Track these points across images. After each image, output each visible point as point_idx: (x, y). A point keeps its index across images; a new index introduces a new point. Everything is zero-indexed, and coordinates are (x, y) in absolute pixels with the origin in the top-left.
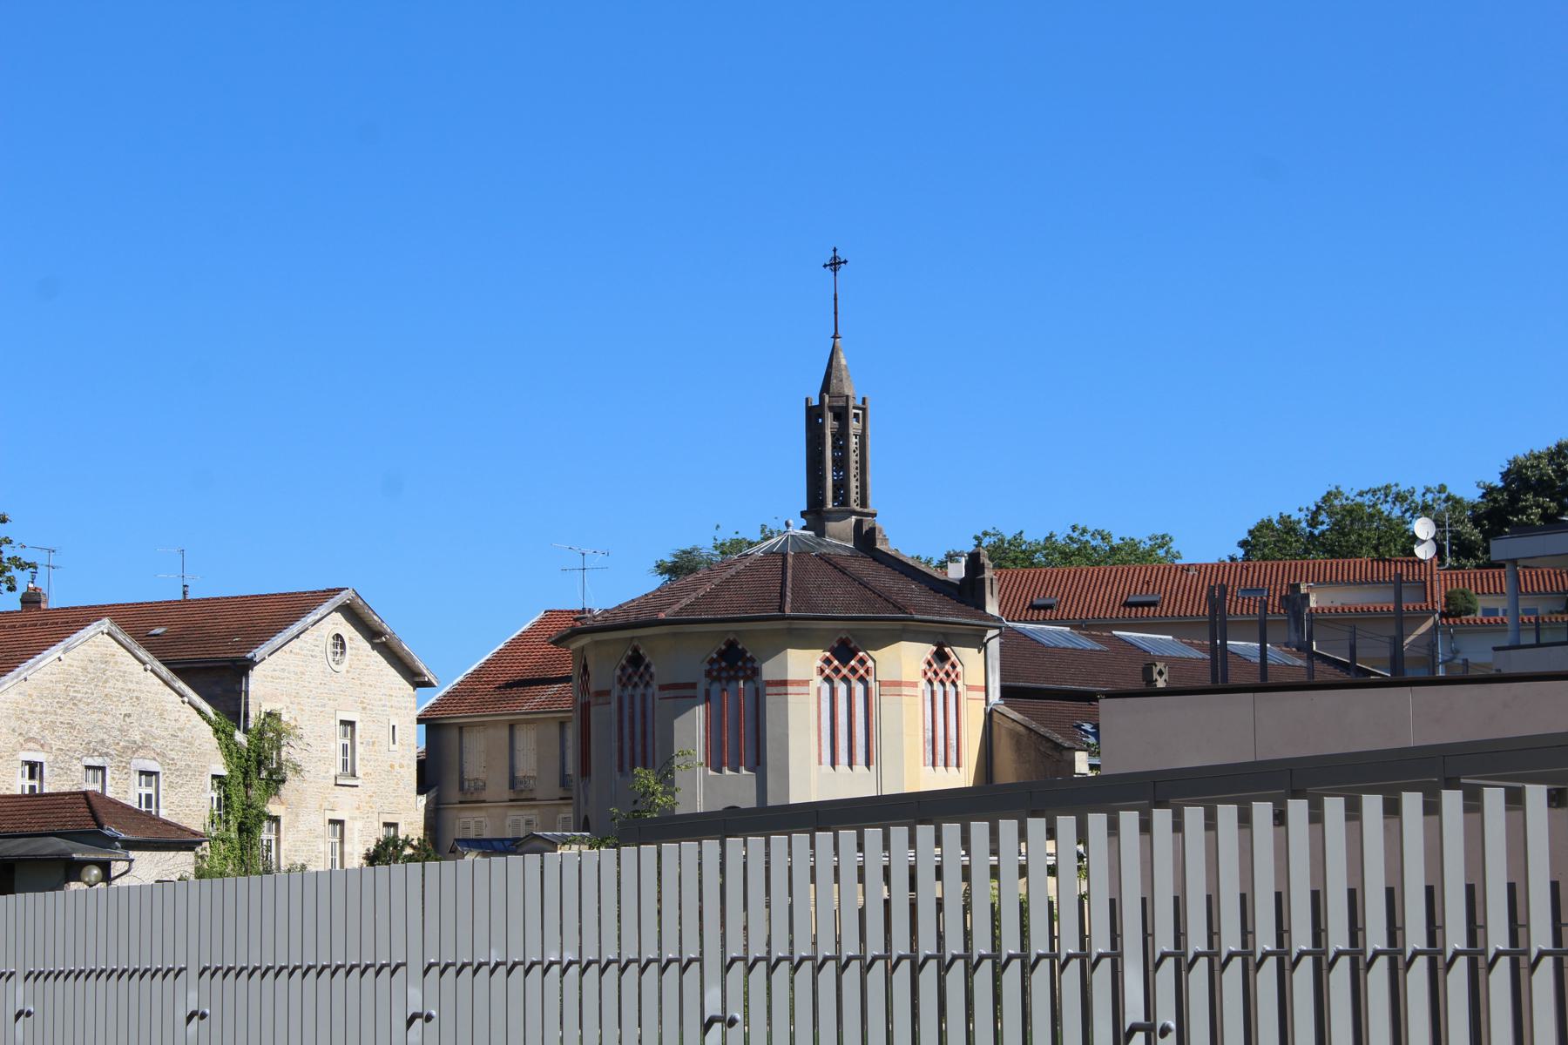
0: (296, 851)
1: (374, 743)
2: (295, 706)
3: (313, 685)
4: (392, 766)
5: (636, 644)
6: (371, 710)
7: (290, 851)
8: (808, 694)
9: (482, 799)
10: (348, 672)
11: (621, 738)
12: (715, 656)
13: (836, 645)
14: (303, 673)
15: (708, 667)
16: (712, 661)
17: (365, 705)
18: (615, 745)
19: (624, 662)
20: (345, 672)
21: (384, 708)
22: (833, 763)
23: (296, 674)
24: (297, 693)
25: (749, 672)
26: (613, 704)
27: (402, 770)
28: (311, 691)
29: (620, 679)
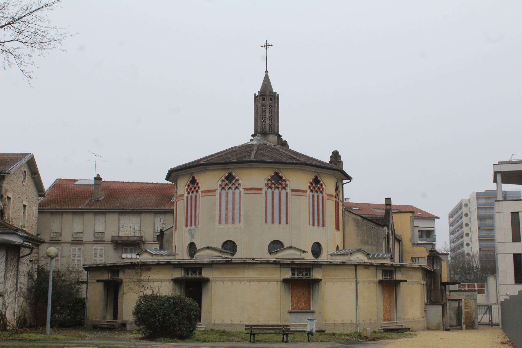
4: (32, 225)
5: (230, 171)
8: (306, 196)
11: (220, 210)
12: (270, 178)
13: (314, 178)
15: (266, 182)
16: (269, 180)
18: (217, 212)
19: (223, 178)
22: (313, 225)
25: (284, 185)
26: (216, 196)
29: (221, 185)
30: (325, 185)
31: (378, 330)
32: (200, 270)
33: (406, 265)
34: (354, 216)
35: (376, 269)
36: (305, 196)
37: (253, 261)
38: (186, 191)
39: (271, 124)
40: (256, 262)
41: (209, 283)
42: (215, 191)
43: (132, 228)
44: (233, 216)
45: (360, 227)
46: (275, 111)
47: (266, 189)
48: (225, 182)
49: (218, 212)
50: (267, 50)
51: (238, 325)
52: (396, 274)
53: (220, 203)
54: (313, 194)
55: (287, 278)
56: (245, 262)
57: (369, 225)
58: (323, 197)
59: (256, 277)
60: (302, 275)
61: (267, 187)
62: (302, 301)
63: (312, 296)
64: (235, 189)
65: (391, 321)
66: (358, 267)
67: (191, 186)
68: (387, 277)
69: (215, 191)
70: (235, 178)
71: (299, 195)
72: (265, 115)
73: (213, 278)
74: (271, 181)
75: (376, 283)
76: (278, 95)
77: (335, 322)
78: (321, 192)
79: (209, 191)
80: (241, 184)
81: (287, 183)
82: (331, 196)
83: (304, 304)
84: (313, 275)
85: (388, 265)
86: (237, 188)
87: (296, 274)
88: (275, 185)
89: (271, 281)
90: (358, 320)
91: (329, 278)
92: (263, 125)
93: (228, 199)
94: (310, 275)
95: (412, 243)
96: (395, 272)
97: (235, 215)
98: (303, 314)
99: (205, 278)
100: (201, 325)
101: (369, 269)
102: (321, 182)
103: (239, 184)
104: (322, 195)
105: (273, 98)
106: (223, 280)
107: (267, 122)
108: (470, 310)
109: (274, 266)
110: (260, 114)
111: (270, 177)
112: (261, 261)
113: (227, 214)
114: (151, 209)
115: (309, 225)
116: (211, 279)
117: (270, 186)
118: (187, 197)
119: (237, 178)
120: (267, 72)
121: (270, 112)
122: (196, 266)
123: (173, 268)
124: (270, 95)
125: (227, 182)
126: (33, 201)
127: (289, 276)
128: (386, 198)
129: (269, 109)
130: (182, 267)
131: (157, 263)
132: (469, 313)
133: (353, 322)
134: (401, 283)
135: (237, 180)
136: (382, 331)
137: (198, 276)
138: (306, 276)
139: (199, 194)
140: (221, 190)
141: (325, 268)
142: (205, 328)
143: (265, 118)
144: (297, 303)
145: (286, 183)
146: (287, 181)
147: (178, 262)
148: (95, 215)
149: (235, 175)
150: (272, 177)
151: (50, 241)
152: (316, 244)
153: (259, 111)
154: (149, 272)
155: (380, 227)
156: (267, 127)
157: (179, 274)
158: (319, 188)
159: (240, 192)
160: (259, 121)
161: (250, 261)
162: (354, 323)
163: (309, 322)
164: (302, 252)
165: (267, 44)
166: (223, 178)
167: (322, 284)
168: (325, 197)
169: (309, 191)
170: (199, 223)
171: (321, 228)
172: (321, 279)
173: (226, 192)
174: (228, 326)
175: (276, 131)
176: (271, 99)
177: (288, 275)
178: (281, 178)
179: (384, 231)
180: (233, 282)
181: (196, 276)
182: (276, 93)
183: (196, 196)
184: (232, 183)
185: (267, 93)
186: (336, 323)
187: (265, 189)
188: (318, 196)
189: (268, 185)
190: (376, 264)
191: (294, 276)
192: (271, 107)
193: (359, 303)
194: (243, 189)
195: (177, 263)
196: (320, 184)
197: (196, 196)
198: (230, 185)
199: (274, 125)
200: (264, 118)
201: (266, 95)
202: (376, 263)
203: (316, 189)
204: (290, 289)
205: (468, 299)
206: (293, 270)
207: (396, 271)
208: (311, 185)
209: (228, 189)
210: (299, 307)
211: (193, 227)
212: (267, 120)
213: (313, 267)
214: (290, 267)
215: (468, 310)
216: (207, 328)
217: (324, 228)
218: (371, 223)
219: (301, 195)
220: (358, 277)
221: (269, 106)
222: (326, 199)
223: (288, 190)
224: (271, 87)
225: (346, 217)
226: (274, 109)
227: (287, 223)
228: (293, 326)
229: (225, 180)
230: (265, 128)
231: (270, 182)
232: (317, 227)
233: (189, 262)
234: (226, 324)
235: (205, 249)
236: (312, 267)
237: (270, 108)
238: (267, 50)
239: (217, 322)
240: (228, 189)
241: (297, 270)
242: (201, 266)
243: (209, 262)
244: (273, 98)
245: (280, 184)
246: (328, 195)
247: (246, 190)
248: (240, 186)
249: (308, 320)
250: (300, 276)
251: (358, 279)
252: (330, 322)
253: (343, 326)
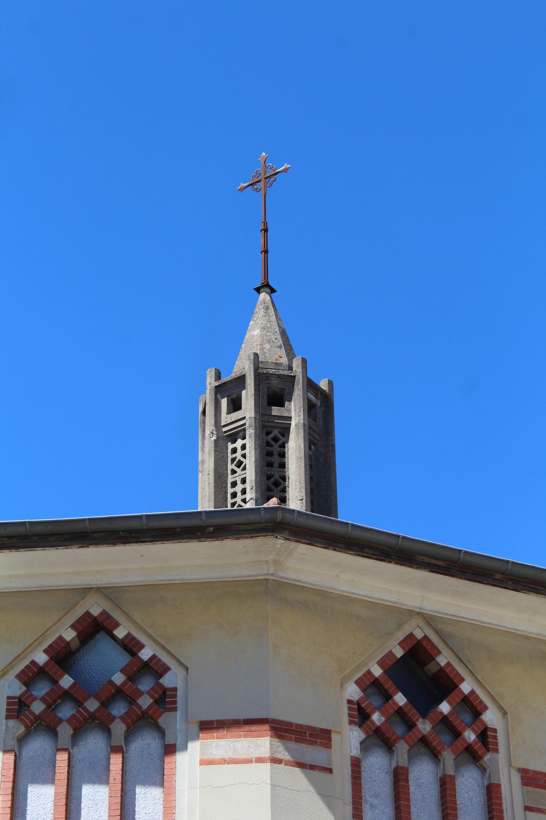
12: (41, 658)
13: (399, 653)
25: (145, 702)
54: (394, 765)
74: (55, 682)
81: (167, 681)
88: (79, 703)
111: (46, 651)
117: (38, 718)
145: (161, 681)
146: (168, 669)
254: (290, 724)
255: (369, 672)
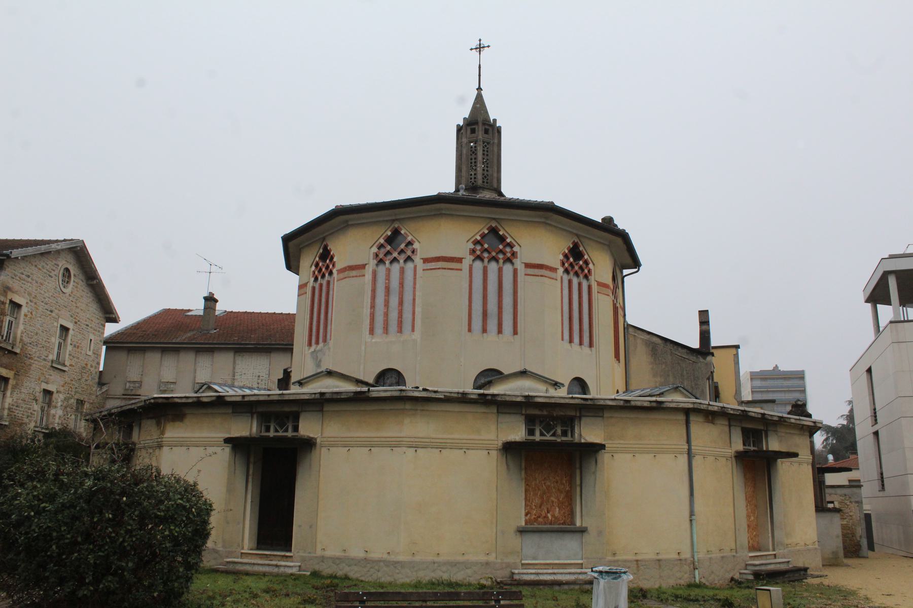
0: (17, 406)
1: (78, 347)
2: (33, 304)
3: (47, 295)
4: (86, 364)
5: (396, 226)
6: (79, 325)
7: (13, 405)
8: (556, 280)
9: (138, 394)
10: (70, 295)
11: (373, 306)
12: (479, 238)
13: (571, 246)
14: (42, 284)
15: (472, 246)
16: (476, 242)
17: (77, 321)
18: (367, 311)
19: (382, 241)
20: (68, 294)
21: (87, 327)
22: (571, 341)
23: (37, 282)
24: (36, 296)
25: (509, 255)
26: (367, 276)
27: (92, 369)
28: (45, 298)
29: (377, 255)
30: (594, 264)
31: (738, 574)
32: (296, 417)
33: (790, 418)
34: (647, 337)
35: (730, 426)
36: (553, 279)
37: (424, 394)
38: (311, 276)
39: (486, 173)
40: (434, 395)
41: (313, 449)
42: (363, 267)
43: (256, 376)
44: (399, 318)
45: (660, 359)
46: (493, 150)
47: (471, 263)
48: (385, 248)
49: (369, 310)
50: (480, 54)
51: (382, 564)
52: (769, 439)
53: (374, 291)
54: (569, 278)
55: (513, 440)
56: (404, 394)
57: (677, 353)
58: (590, 287)
59: (434, 436)
60: (554, 435)
61: (472, 258)
62: (553, 502)
63: (578, 489)
64: (405, 261)
65: (760, 550)
66: (692, 418)
67: (320, 264)
68: (749, 445)
69: (363, 267)
70: (406, 238)
71: (542, 276)
72: (475, 159)
73: (322, 440)
74: (482, 245)
75: (730, 459)
76: (500, 127)
77: (639, 557)
78: (586, 277)
79: (351, 268)
80: (418, 251)
81: (515, 249)
82: (606, 286)
83: (557, 509)
84: (580, 435)
85: (756, 416)
86: (409, 259)
87: (537, 433)
88: (489, 253)
89: (472, 449)
90: (695, 550)
91: (622, 442)
92: (471, 175)
93: (389, 283)
94: (572, 436)
95: (738, 401)
96: (767, 436)
97: (404, 316)
98: (554, 535)
99: (306, 437)
100: (291, 560)
101: (714, 424)
102: (586, 257)
103: (413, 252)
104: (588, 284)
105: (490, 129)
106: (347, 445)
107: (478, 169)
108: (851, 521)
109: (481, 409)
110: (467, 155)
111: (480, 236)
112: (446, 394)
113: (386, 315)
114: (286, 345)
115: (563, 339)
116: (318, 441)
118: (314, 288)
119: (409, 238)
120: (479, 89)
121: (486, 153)
122: (287, 409)
123: (233, 412)
124: (484, 124)
125: (389, 248)
126: (90, 326)
127: (520, 436)
128: (699, 311)
129: (483, 147)
130: (254, 411)
131: (195, 400)
132: (849, 527)
133: (683, 556)
134: (779, 460)
135: (410, 243)
136: (751, 577)
137: (290, 434)
138: (564, 439)
139: (334, 278)
140: (377, 265)
141: (611, 417)
142: (300, 566)
143: (475, 162)
144: (540, 507)
145: (513, 249)
147: (241, 397)
148: (196, 355)
149: (405, 233)
150: (483, 236)
151: (123, 395)
152: (576, 382)
153: (464, 151)
154: (181, 423)
155: (699, 356)
156: (480, 177)
157: (245, 428)
158: (581, 268)
159: (415, 267)
160: (464, 169)
161: (416, 394)
162: (686, 560)
163: (602, 582)
164: (551, 384)
165: (480, 44)
166: (382, 241)
167: (604, 457)
168: (593, 286)
169: (561, 270)
170: (331, 336)
171: (586, 349)
172: (603, 443)
173: (387, 269)
174: (355, 565)
175: (495, 186)
176: (486, 132)
177: (517, 433)
178: (502, 239)
179: (707, 364)
180: (372, 448)
181: (285, 434)
182: (495, 120)
183: (328, 282)
184: (399, 250)
185: (480, 120)
186: (640, 561)
187: (468, 259)
188: (580, 284)
189: (475, 252)
190: (732, 412)
191: (531, 438)
192: (486, 144)
193: (697, 508)
194: (422, 261)
195: (239, 399)
196: (583, 260)
197: (328, 282)
198: (395, 254)
199: (493, 174)
200: (473, 163)
201: (476, 123)
202: (731, 409)
203: (576, 268)
204: (521, 469)
205: (846, 502)
206: (530, 422)
207: (769, 433)
208: (565, 260)
209: (391, 262)
210: (546, 517)
211: (321, 345)
212: (479, 165)
213: (580, 413)
214: (522, 415)
215: (847, 521)
216: (303, 567)
217: (593, 349)
218: (680, 349)
219: (546, 277)
220: (693, 443)
221: (483, 144)
222: (596, 292)
223: (518, 263)
224: (487, 112)
225: (631, 339)
226: (491, 149)
227: (515, 332)
228: (531, 567)
229: (386, 245)
230: (476, 180)
231: (478, 247)
232: (579, 347)
233: (266, 398)
234: (352, 559)
235: (323, 376)
236: (578, 415)
237: (486, 146)
238: (480, 54)
239: (328, 553)
240: (391, 262)
241: (541, 422)
242: (294, 409)
243: (313, 396)
244: (490, 129)
245: (501, 251)
246: (600, 284)
247: (428, 262)
248: (416, 255)
249: (596, 575)
250: (548, 437)
251: (693, 448)
252: (625, 557)
253: (660, 566)
254: (548, 266)
255: (565, 252)
